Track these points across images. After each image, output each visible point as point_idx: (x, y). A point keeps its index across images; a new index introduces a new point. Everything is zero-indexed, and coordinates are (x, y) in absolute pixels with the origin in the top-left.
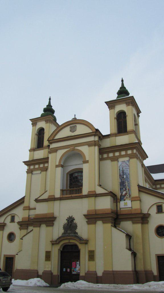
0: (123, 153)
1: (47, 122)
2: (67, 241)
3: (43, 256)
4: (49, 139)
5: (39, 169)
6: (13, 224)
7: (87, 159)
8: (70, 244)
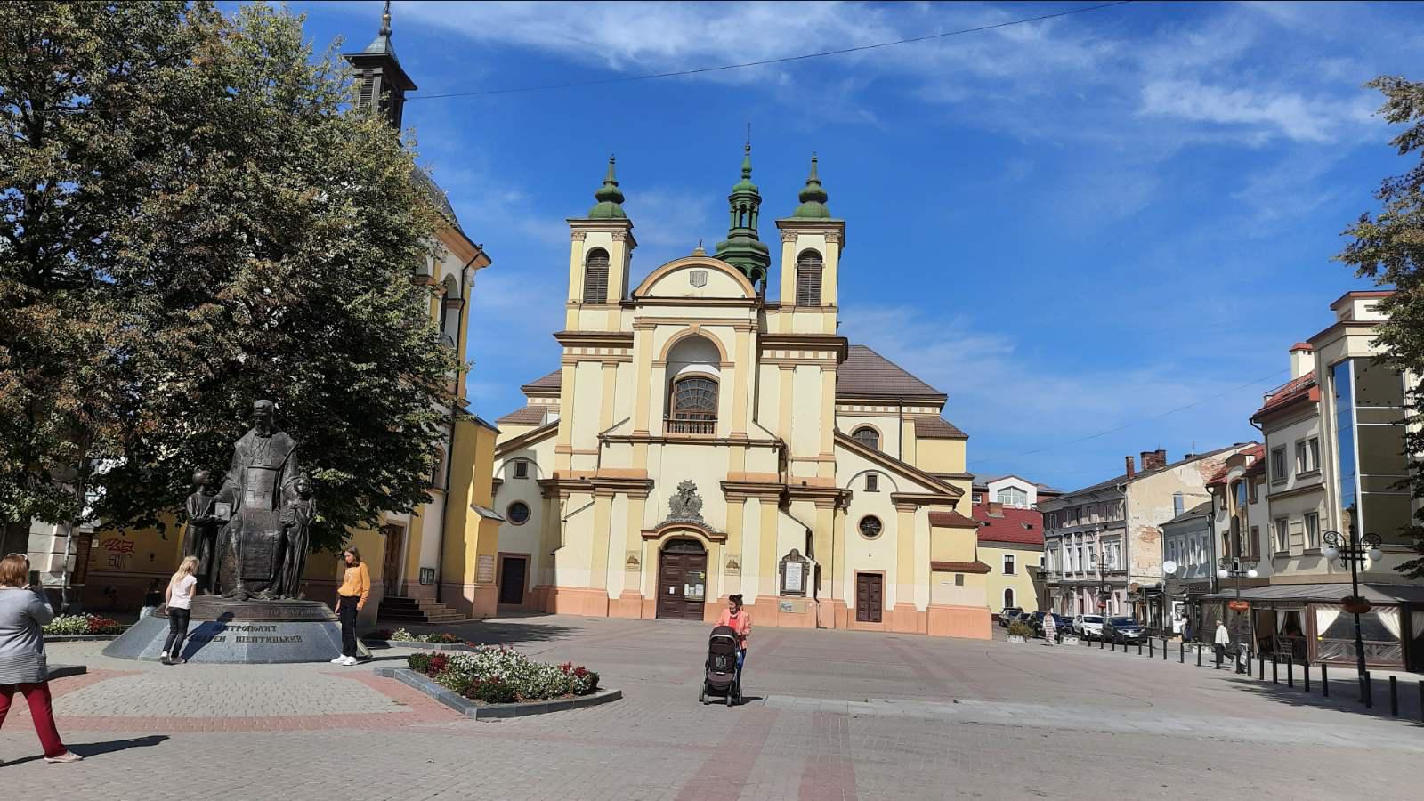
0: (809, 354)
4: (636, 295)
8: (683, 538)
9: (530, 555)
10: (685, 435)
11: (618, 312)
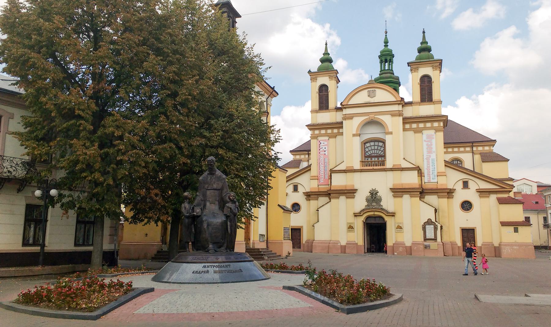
0: (429, 125)
1: (330, 77)
2: (372, 213)
3: (345, 227)
4: (343, 104)
5: (325, 135)
6: (296, 193)
7: (390, 131)
9: (302, 227)
10: (371, 168)
11: (334, 113)
